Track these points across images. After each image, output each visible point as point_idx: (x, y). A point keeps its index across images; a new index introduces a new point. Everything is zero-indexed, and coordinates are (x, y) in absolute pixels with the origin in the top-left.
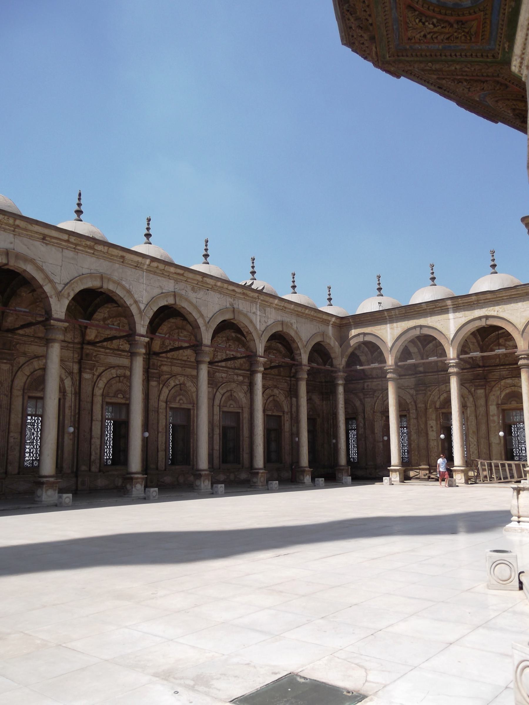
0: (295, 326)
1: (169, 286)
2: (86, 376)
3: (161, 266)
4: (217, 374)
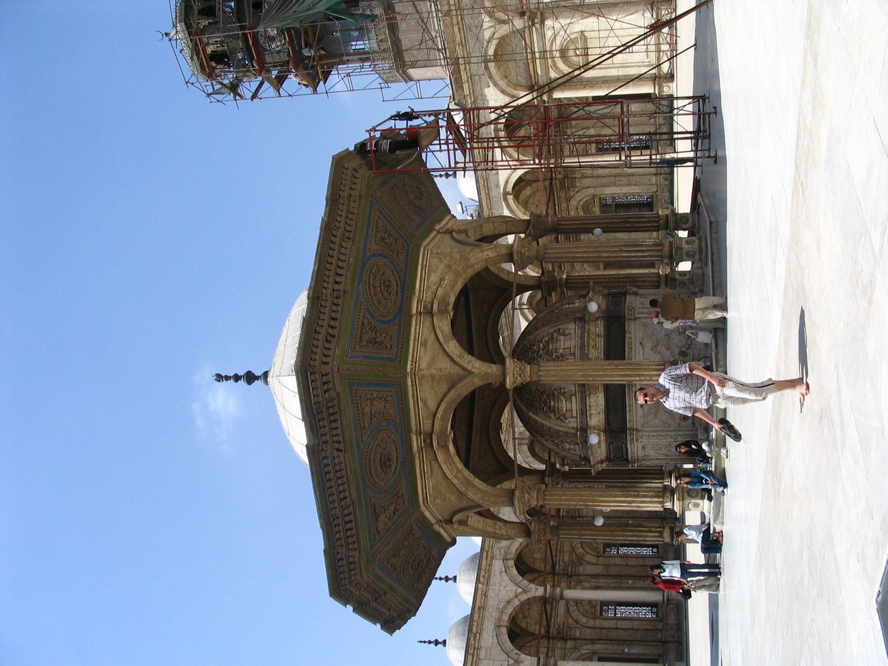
1: (498, 565)
3: (483, 573)
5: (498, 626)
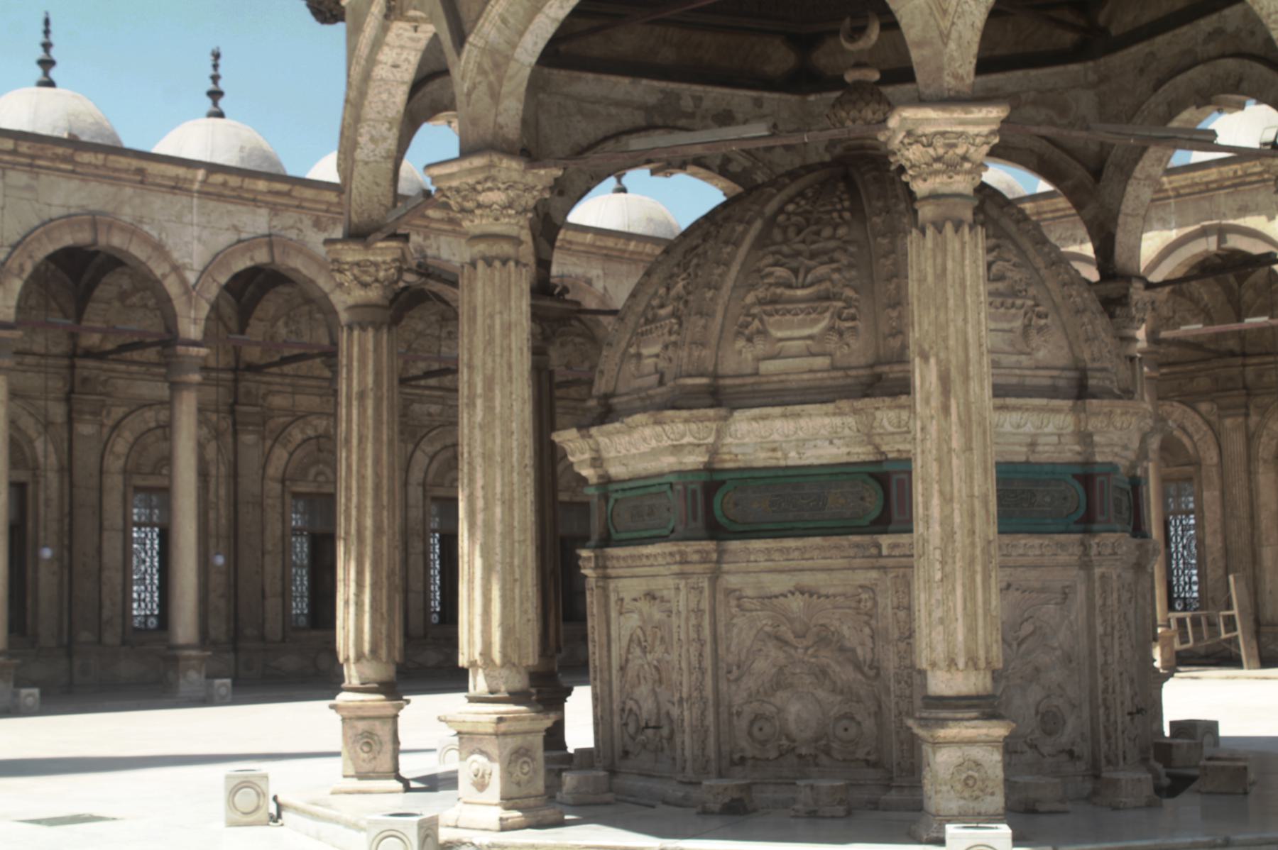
0: (599, 286)
1: (257, 222)
2: (85, 429)
3: (234, 181)
4: (416, 407)
5: (95, 220)
